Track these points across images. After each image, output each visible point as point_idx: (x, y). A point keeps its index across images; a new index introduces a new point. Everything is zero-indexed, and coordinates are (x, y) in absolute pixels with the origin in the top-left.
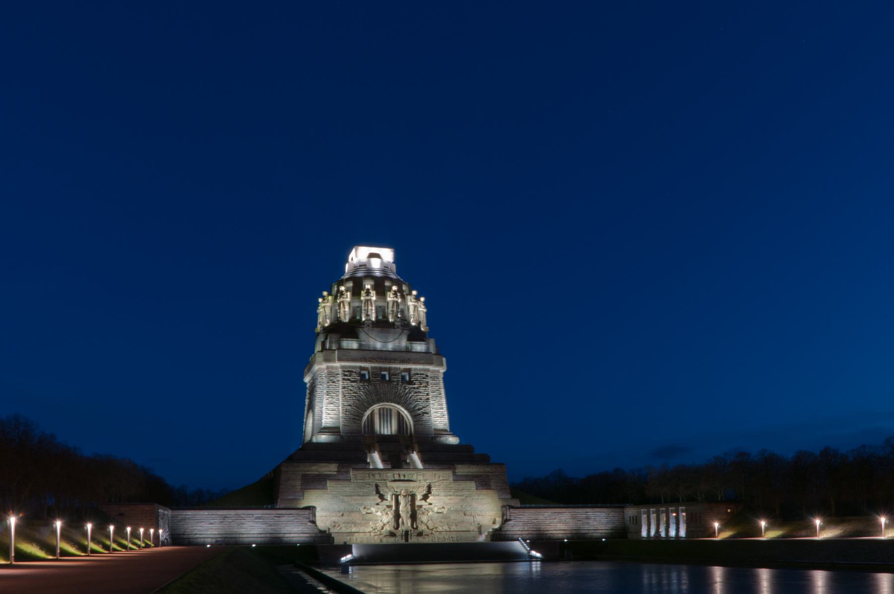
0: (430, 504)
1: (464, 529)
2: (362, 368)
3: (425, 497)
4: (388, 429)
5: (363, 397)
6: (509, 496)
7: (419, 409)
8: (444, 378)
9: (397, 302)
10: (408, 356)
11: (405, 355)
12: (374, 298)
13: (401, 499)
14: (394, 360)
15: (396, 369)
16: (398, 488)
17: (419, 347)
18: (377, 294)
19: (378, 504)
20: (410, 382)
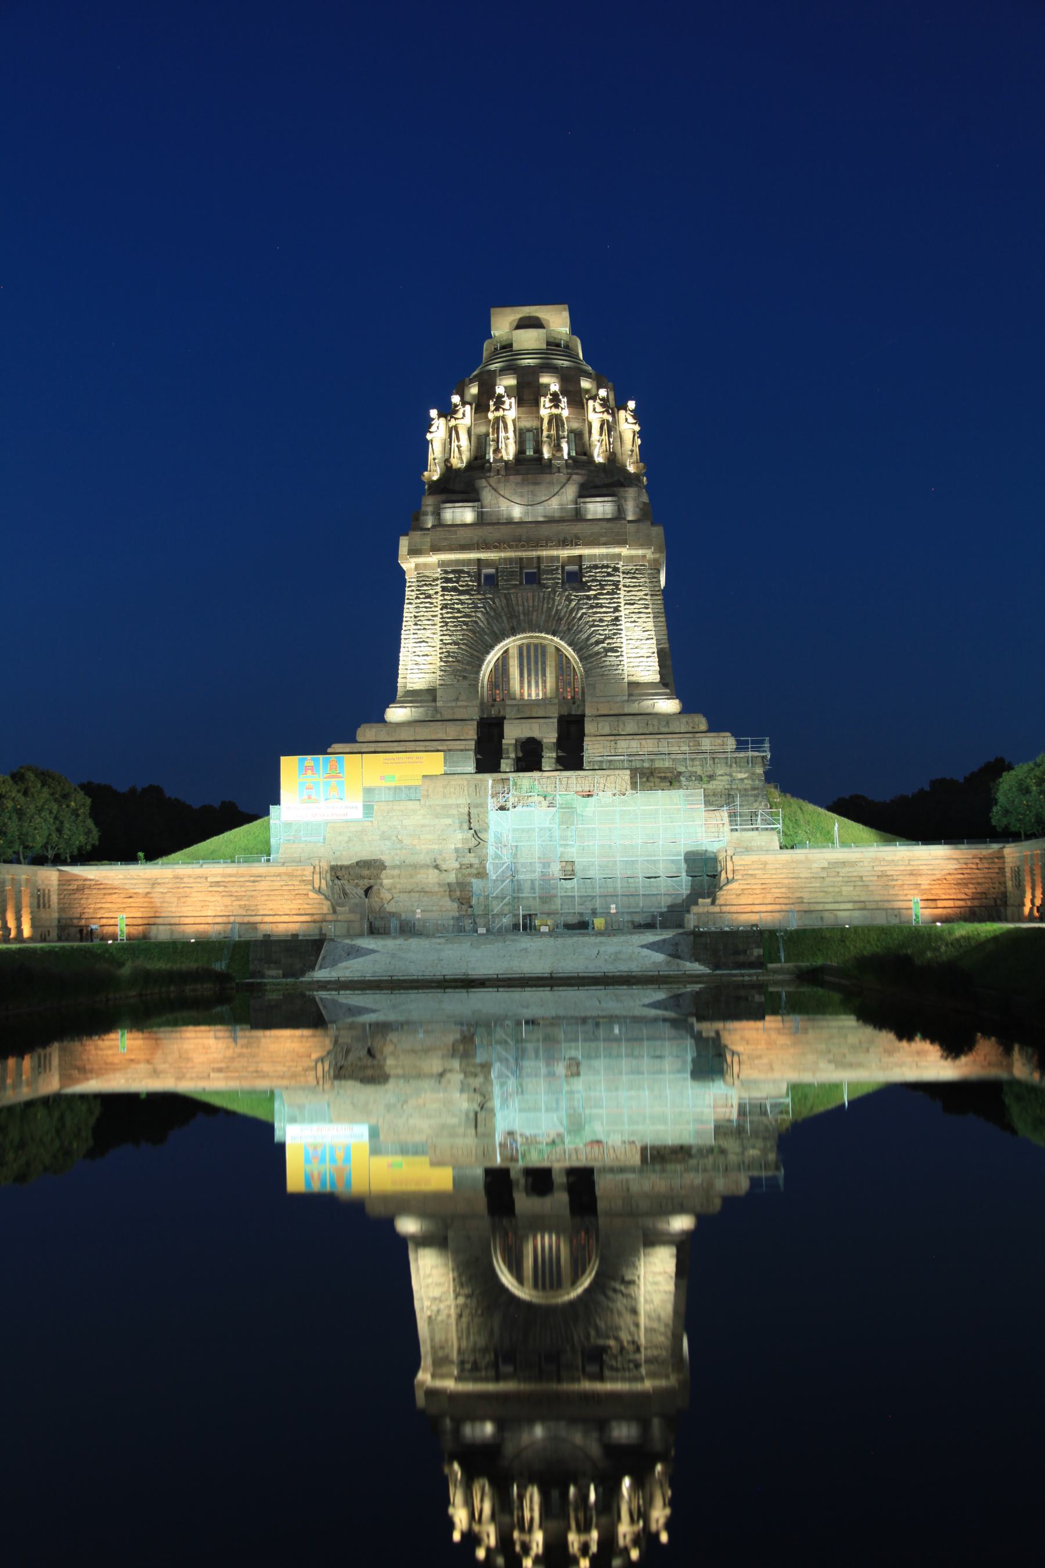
7: (597, 643)
10: (577, 528)
18: (520, 403)
20: (584, 587)
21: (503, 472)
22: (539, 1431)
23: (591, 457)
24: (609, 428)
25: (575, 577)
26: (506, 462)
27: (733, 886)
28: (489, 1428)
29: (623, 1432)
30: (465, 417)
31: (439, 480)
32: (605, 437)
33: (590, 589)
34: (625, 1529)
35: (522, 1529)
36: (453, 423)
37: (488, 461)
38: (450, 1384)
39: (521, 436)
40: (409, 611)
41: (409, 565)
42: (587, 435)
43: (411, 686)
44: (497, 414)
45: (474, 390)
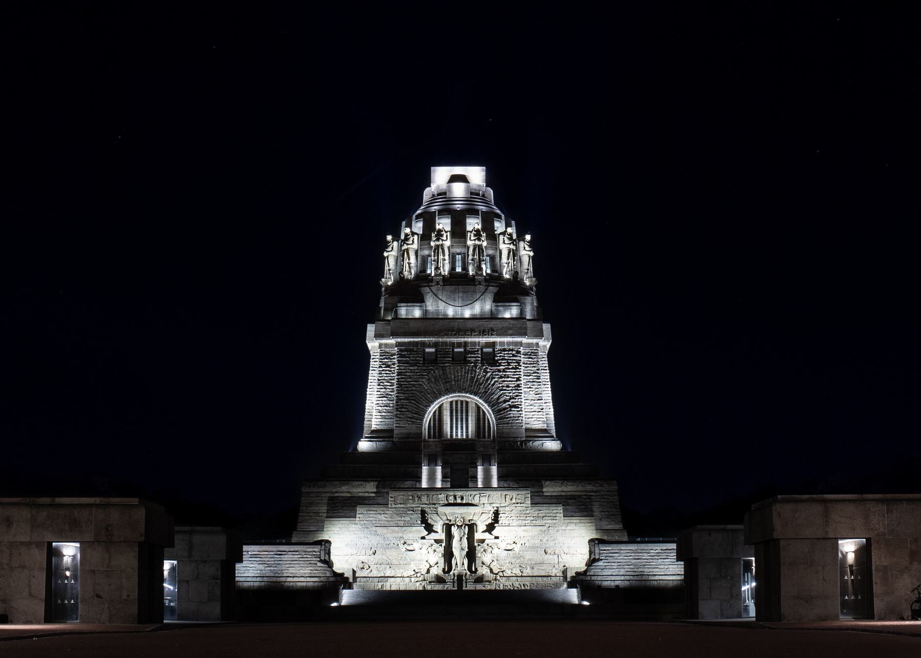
0: (497, 538)
3: (490, 528)
4: (460, 430)
6: (619, 526)
7: (505, 401)
8: (549, 355)
9: (480, 247)
10: (492, 324)
11: (487, 324)
14: (471, 332)
15: (474, 344)
17: (511, 312)
19: (423, 538)
21: (441, 283)
23: (501, 274)
24: (514, 254)
25: (490, 358)
26: (444, 276)
27: (600, 563)
31: (392, 285)
32: (511, 261)
33: (500, 365)
36: (405, 247)
37: (430, 274)
41: (373, 345)
42: (498, 259)
44: (437, 243)
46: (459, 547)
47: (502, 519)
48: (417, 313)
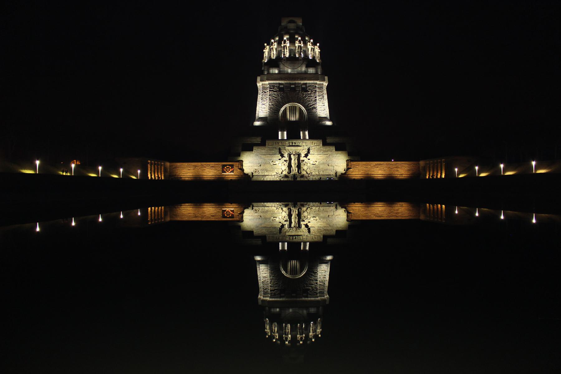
1: (327, 174)
2: (279, 84)
3: (306, 156)
4: (293, 118)
5: (280, 100)
10: (305, 76)
12: (288, 45)
13: (292, 156)
16: (291, 150)
20: (307, 91)
22: (291, 310)
24: (313, 50)
25: (305, 89)
27: (351, 170)
28: (278, 310)
29: (312, 310)
30: (275, 46)
34: (311, 334)
35: (286, 334)
38: (268, 299)
39: (291, 51)
40: (260, 96)
41: (259, 84)
43: (260, 116)
45: (277, 39)
46: (294, 163)
47: (311, 152)
48: (277, 71)
